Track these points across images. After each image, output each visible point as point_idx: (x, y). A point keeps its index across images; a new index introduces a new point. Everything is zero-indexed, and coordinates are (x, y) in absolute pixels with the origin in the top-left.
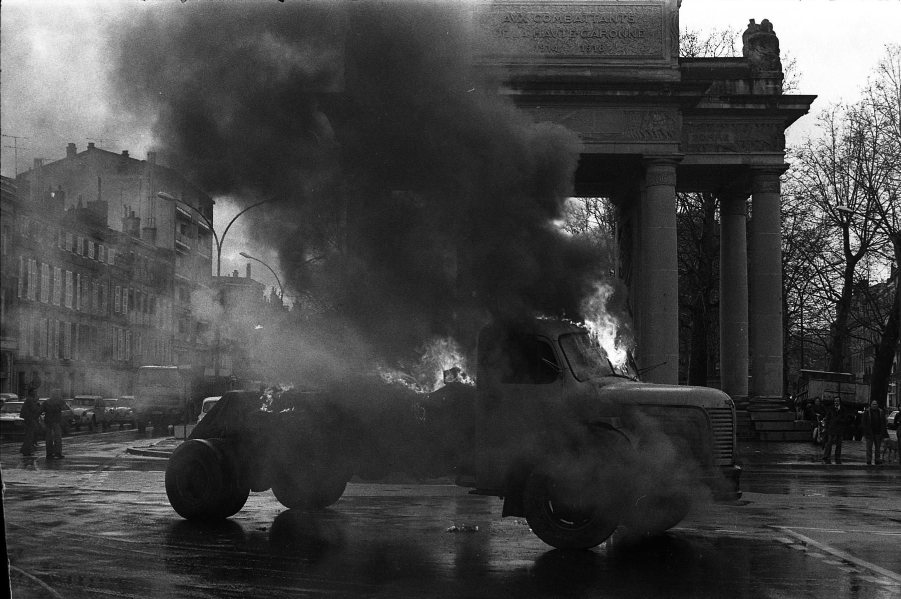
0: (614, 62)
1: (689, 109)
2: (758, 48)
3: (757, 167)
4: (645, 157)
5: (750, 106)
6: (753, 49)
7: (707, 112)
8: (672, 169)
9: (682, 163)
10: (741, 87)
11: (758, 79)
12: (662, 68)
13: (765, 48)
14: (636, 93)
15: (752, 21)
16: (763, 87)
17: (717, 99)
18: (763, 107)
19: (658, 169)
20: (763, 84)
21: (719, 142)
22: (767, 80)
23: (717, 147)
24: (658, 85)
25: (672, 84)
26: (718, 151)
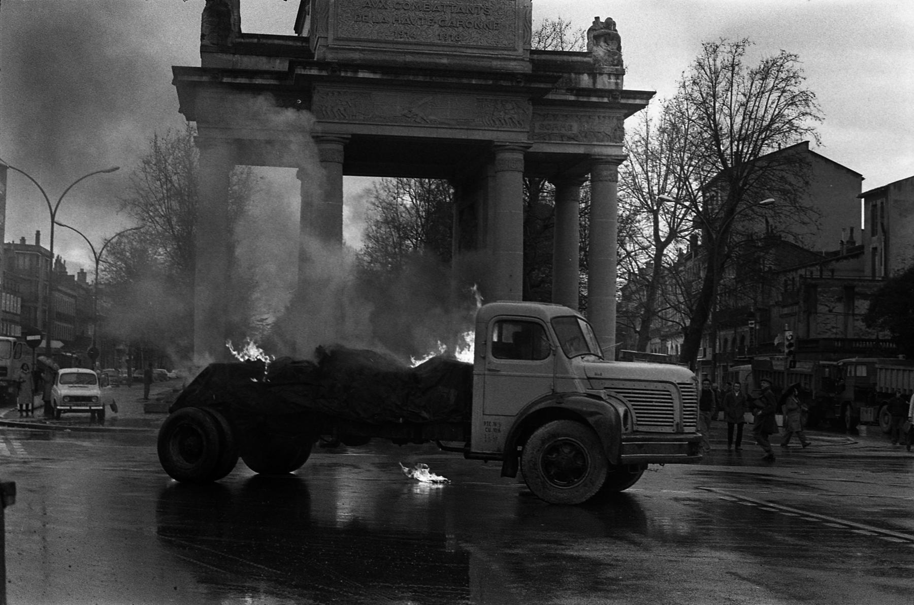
0: (469, 51)
2: (602, 43)
6: (597, 44)
7: (553, 103)
9: (531, 150)
12: (515, 60)
13: (608, 44)
14: (491, 82)
15: (597, 18)
16: (605, 82)
19: (507, 155)
24: (511, 76)
26: (562, 140)
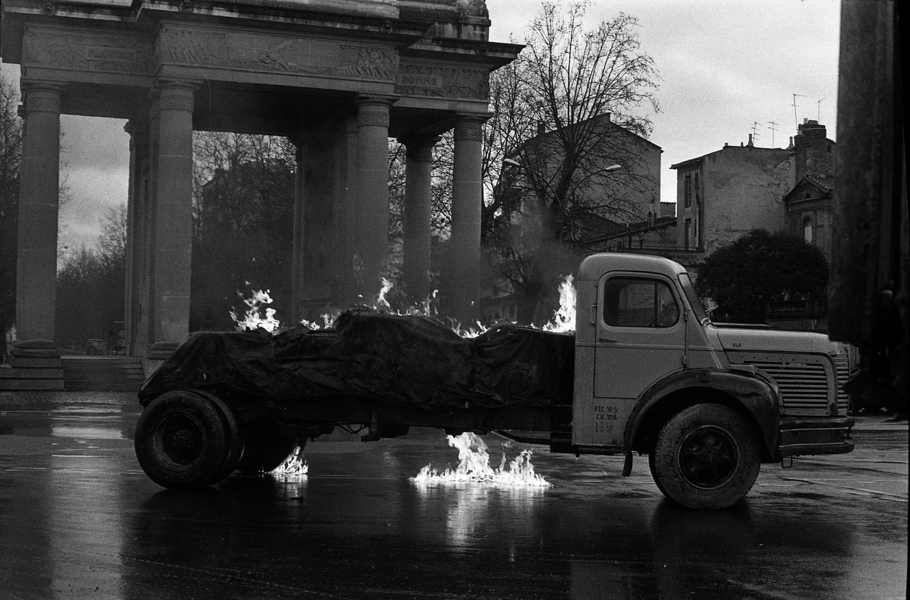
1: (404, 50)
3: (462, 114)
4: (361, 95)
5: (461, 51)
8: (387, 111)
10: (450, 31)
11: (466, 24)
14: (356, 27)
16: (470, 33)
17: (430, 41)
18: (472, 52)
20: (471, 28)
21: (427, 85)
22: (475, 26)
23: (426, 91)
24: (378, 20)
25: (393, 21)
